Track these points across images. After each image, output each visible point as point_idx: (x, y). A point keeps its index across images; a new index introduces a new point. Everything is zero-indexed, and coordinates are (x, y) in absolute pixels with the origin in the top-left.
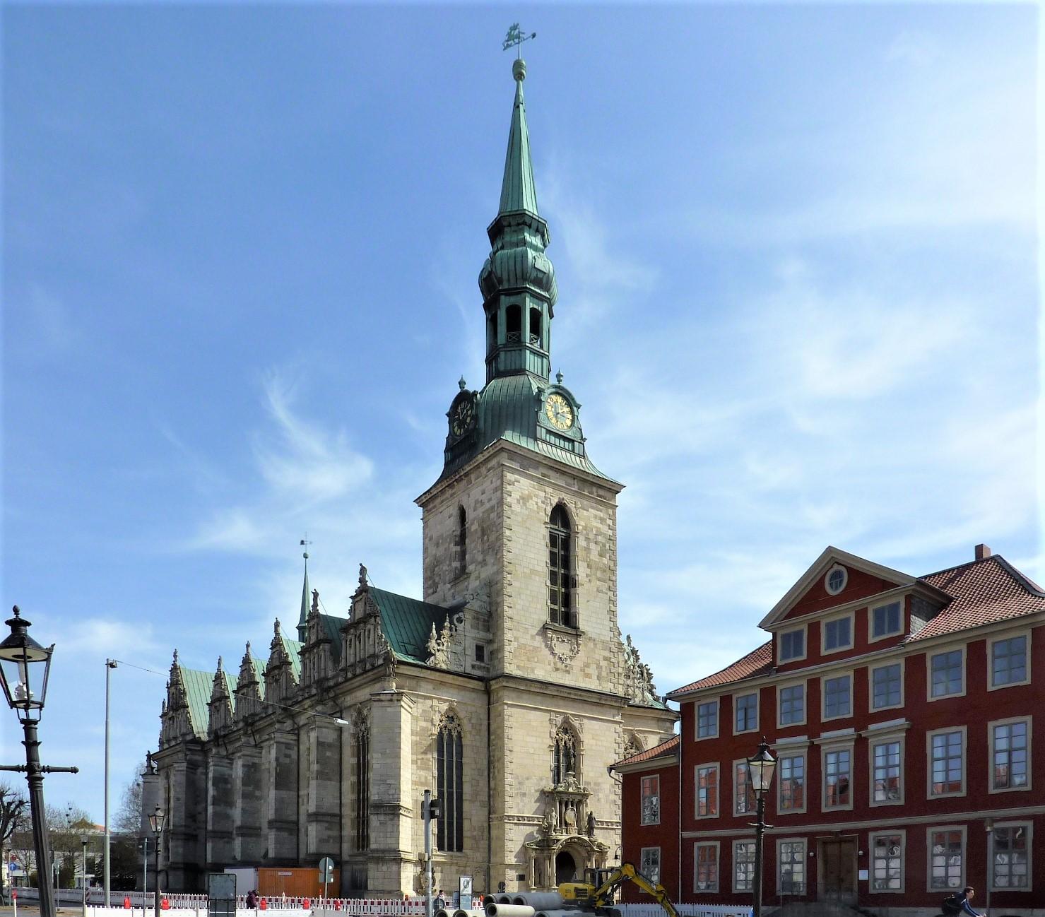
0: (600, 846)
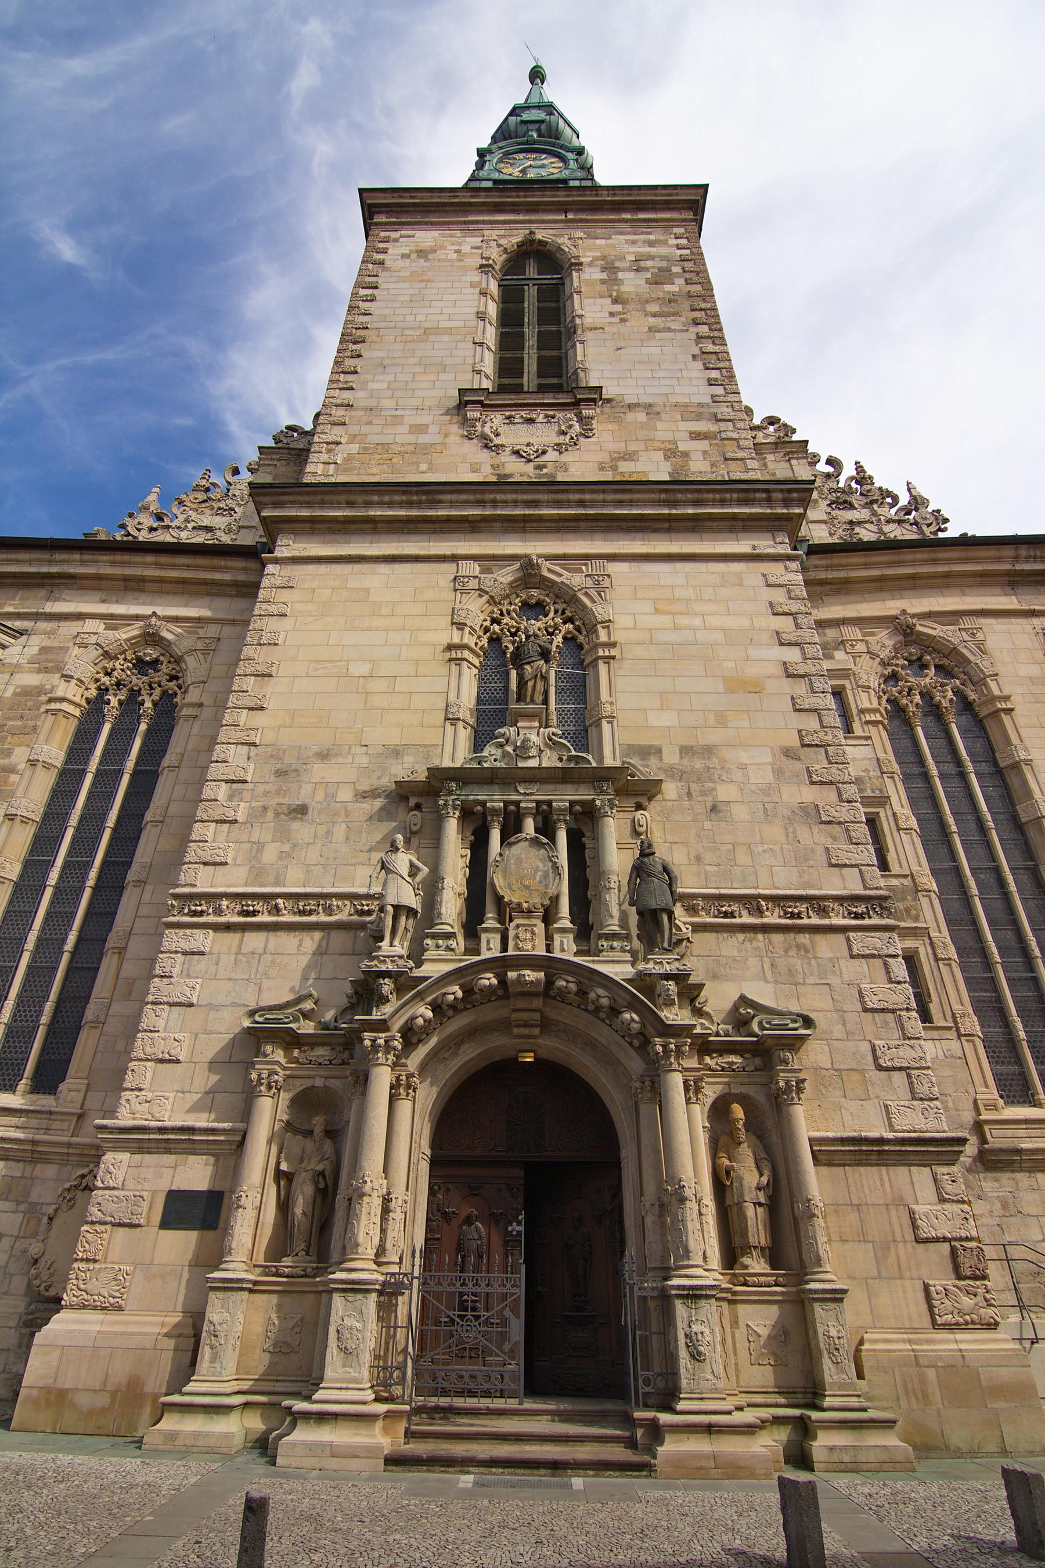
0: (743, 1012)
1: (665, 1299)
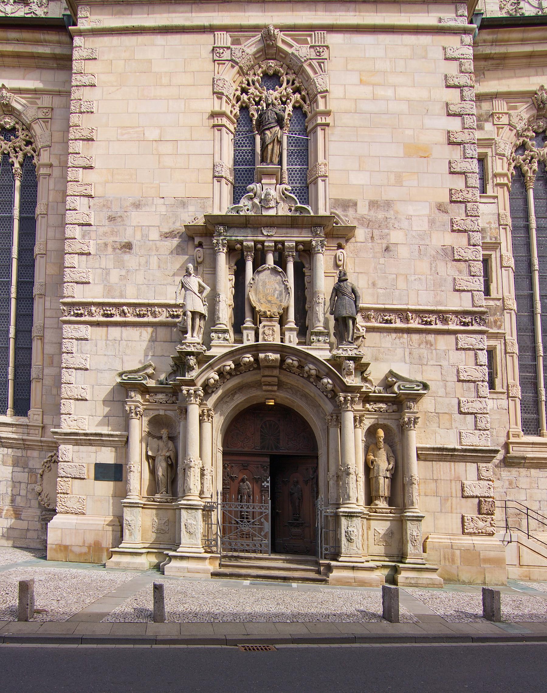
1: (337, 517)
